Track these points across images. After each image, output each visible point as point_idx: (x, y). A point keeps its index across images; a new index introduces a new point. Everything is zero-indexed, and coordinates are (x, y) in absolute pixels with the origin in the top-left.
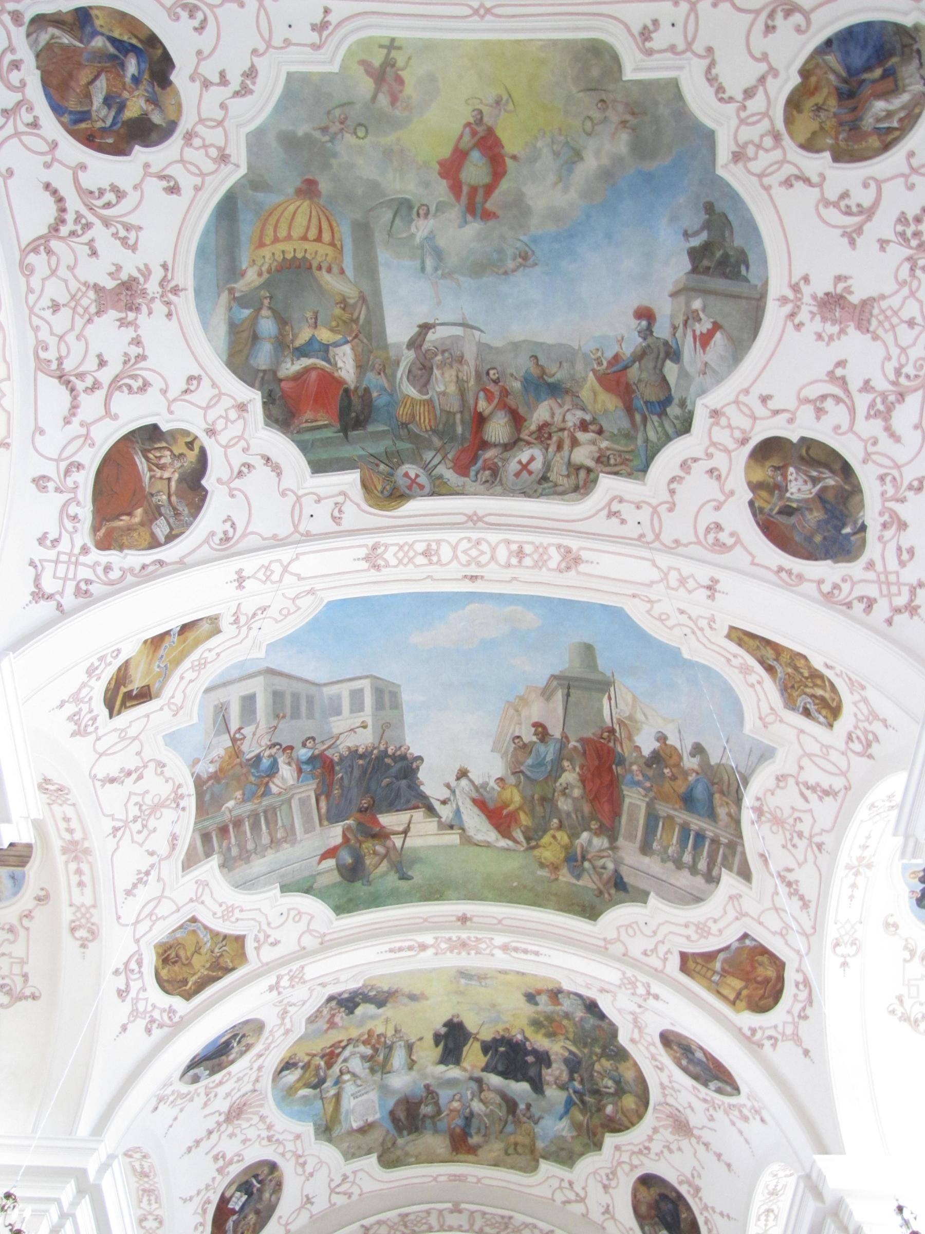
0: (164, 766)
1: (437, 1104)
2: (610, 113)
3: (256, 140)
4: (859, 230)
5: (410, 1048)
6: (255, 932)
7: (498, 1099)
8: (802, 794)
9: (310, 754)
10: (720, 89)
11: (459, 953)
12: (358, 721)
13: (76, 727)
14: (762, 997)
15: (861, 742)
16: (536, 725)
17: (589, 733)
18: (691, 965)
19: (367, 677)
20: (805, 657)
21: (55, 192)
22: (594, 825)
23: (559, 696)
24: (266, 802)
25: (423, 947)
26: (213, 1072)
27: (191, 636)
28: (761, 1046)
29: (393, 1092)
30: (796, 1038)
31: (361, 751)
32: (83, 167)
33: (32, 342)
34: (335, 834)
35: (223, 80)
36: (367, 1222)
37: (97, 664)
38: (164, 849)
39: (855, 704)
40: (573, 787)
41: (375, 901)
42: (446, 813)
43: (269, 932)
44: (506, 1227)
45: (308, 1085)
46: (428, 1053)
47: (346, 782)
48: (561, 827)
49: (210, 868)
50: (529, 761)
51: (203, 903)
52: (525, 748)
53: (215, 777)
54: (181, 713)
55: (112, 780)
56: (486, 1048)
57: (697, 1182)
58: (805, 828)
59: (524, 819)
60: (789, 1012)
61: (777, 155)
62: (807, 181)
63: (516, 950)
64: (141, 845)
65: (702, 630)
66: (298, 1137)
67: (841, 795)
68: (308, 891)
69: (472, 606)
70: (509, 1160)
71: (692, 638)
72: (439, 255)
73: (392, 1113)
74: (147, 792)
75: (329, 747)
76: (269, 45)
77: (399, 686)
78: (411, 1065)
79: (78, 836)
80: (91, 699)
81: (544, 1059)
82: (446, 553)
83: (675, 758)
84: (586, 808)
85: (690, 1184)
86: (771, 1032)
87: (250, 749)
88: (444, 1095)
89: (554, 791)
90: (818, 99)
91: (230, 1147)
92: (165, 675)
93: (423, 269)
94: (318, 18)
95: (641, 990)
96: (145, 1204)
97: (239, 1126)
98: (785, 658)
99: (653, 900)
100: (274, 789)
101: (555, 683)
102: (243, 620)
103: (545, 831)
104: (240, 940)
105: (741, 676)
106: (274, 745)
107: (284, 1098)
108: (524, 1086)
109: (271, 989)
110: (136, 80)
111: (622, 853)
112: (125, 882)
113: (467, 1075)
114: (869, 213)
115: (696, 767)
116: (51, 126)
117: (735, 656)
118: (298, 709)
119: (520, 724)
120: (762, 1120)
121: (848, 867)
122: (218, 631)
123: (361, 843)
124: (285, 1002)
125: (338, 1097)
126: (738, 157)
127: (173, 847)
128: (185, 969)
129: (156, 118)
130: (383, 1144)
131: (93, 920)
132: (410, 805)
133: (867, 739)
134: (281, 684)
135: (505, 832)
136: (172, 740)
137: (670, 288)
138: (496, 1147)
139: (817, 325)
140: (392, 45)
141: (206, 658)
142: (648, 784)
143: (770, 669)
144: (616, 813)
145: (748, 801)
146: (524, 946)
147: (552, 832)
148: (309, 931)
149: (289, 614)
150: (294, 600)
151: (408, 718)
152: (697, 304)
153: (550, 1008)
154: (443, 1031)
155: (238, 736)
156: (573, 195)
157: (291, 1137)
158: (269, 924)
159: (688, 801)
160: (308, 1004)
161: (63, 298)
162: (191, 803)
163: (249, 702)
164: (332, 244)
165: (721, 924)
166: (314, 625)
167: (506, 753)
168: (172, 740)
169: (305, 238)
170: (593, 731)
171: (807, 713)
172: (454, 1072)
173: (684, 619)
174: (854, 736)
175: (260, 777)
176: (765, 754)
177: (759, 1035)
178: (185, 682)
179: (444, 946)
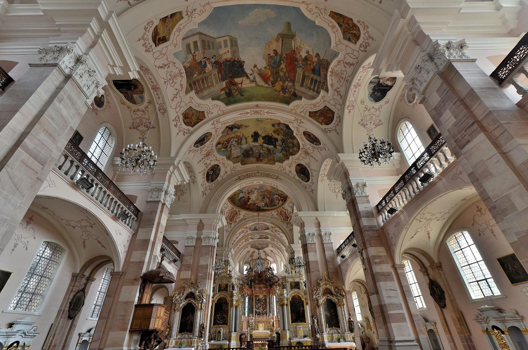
0: (175, 63)
1: (253, 151)
5: (246, 139)
6: (207, 110)
7: (266, 150)
8: (344, 66)
13: (146, 49)
14: (328, 121)
15: (364, 47)
16: (274, 50)
18: (312, 114)
19: (228, 36)
20: (352, 19)
22: (289, 79)
23: (281, 40)
24: (205, 75)
25: (248, 113)
26: (201, 145)
27: (175, 18)
28: (327, 132)
29: (243, 149)
30: (335, 130)
31: (228, 60)
34: (224, 84)
36: (239, 176)
37: (147, 26)
38: (180, 88)
39: (364, 34)
40: (284, 69)
41: (235, 102)
42: (251, 77)
43: (210, 110)
44: (269, 175)
45: (223, 148)
46: (250, 140)
47: (225, 69)
48: (281, 80)
49: (193, 93)
50: (272, 62)
51: (192, 103)
53: (190, 67)
54: (177, 46)
55: (161, 67)
56: (263, 138)
57: (310, 164)
58: (344, 76)
59: (271, 79)
60: (334, 124)
63: (269, 113)
64: (173, 87)
65: (322, 13)
66: (223, 159)
67: (355, 65)
68: (218, 100)
70: (269, 163)
73: (243, 153)
74: (172, 71)
78: (247, 143)
79: (155, 84)
80: (148, 39)
81: (276, 140)
84: (287, 75)
85: (308, 165)
86: (330, 129)
87: (199, 59)
88: (254, 149)
89: (279, 70)
91: (208, 162)
92: (170, 34)
95: (299, 121)
96: (191, 174)
97: (209, 157)
98: (346, 20)
99: (303, 99)
100: (207, 71)
102: (189, 14)
103: (276, 82)
104: (203, 112)
105: (332, 29)
106: (205, 58)
107: (218, 151)
108: (272, 146)
109: (212, 124)
111: (296, 87)
112: (171, 97)
113: (259, 144)
115: (316, 61)
117: (331, 22)
118: (210, 46)
120: (325, 150)
121: (354, 86)
122: (182, 18)
123: (230, 86)
124: (216, 128)
125: (231, 150)
127: (182, 88)
128: (190, 120)
130: (241, 160)
131: (164, 107)
132: (242, 76)
133: (366, 46)
134: (204, 38)
135: (266, 82)
136: (176, 55)
138: (266, 160)
141: (180, 28)
142: (303, 67)
143: (340, 26)
144: (295, 76)
145: (330, 70)
147: (278, 82)
148: (220, 110)
149: (203, 12)
151: (240, 49)
153: (278, 128)
154: (253, 134)
155: (194, 55)
157: (221, 159)
158: (210, 108)
159: (314, 71)
160: (222, 129)
162: (184, 75)
163: (195, 43)
165: (319, 104)
166: (211, 17)
167: (266, 59)
168: (176, 55)
171: (349, 40)
172: (256, 144)
173: (317, 10)
174: (362, 45)
175: (202, 67)
176: (336, 55)
177: (327, 130)
178: (176, 36)
179: (252, 113)
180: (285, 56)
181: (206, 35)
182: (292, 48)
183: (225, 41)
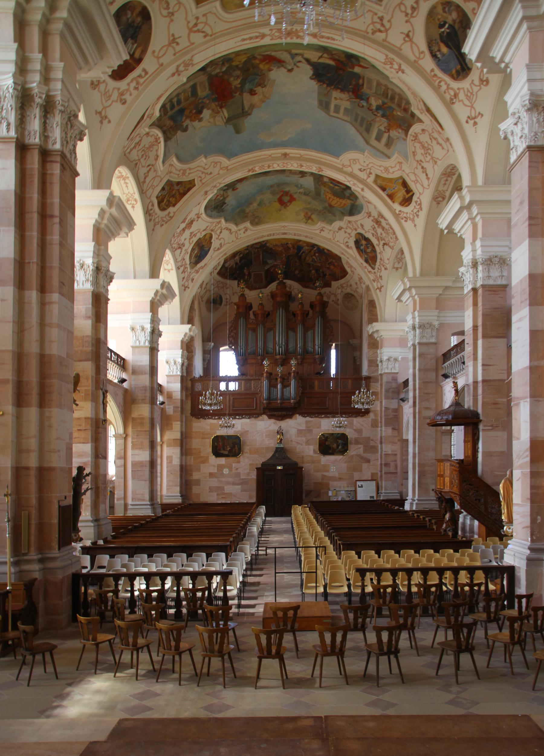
3: (341, 219)
9: (362, 101)
11: (292, 29)
16: (255, 94)
23: (246, 108)
27: (384, 184)
31: (339, 91)
35: (346, 232)
48: (237, 66)
52: (259, 85)
55: (427, 175)
63: (257, 37)
72: (297, 186)
94: (322, 232)
101: (249, 112)
106: (375, 115)
116: (379, 256)
129: (361, 237)
136: (406, 157)
140: (306, 223)
146: (252, 41)
150: (350, 166)
151: (315, 95)
161: (389, 238)
181: (361, 134)
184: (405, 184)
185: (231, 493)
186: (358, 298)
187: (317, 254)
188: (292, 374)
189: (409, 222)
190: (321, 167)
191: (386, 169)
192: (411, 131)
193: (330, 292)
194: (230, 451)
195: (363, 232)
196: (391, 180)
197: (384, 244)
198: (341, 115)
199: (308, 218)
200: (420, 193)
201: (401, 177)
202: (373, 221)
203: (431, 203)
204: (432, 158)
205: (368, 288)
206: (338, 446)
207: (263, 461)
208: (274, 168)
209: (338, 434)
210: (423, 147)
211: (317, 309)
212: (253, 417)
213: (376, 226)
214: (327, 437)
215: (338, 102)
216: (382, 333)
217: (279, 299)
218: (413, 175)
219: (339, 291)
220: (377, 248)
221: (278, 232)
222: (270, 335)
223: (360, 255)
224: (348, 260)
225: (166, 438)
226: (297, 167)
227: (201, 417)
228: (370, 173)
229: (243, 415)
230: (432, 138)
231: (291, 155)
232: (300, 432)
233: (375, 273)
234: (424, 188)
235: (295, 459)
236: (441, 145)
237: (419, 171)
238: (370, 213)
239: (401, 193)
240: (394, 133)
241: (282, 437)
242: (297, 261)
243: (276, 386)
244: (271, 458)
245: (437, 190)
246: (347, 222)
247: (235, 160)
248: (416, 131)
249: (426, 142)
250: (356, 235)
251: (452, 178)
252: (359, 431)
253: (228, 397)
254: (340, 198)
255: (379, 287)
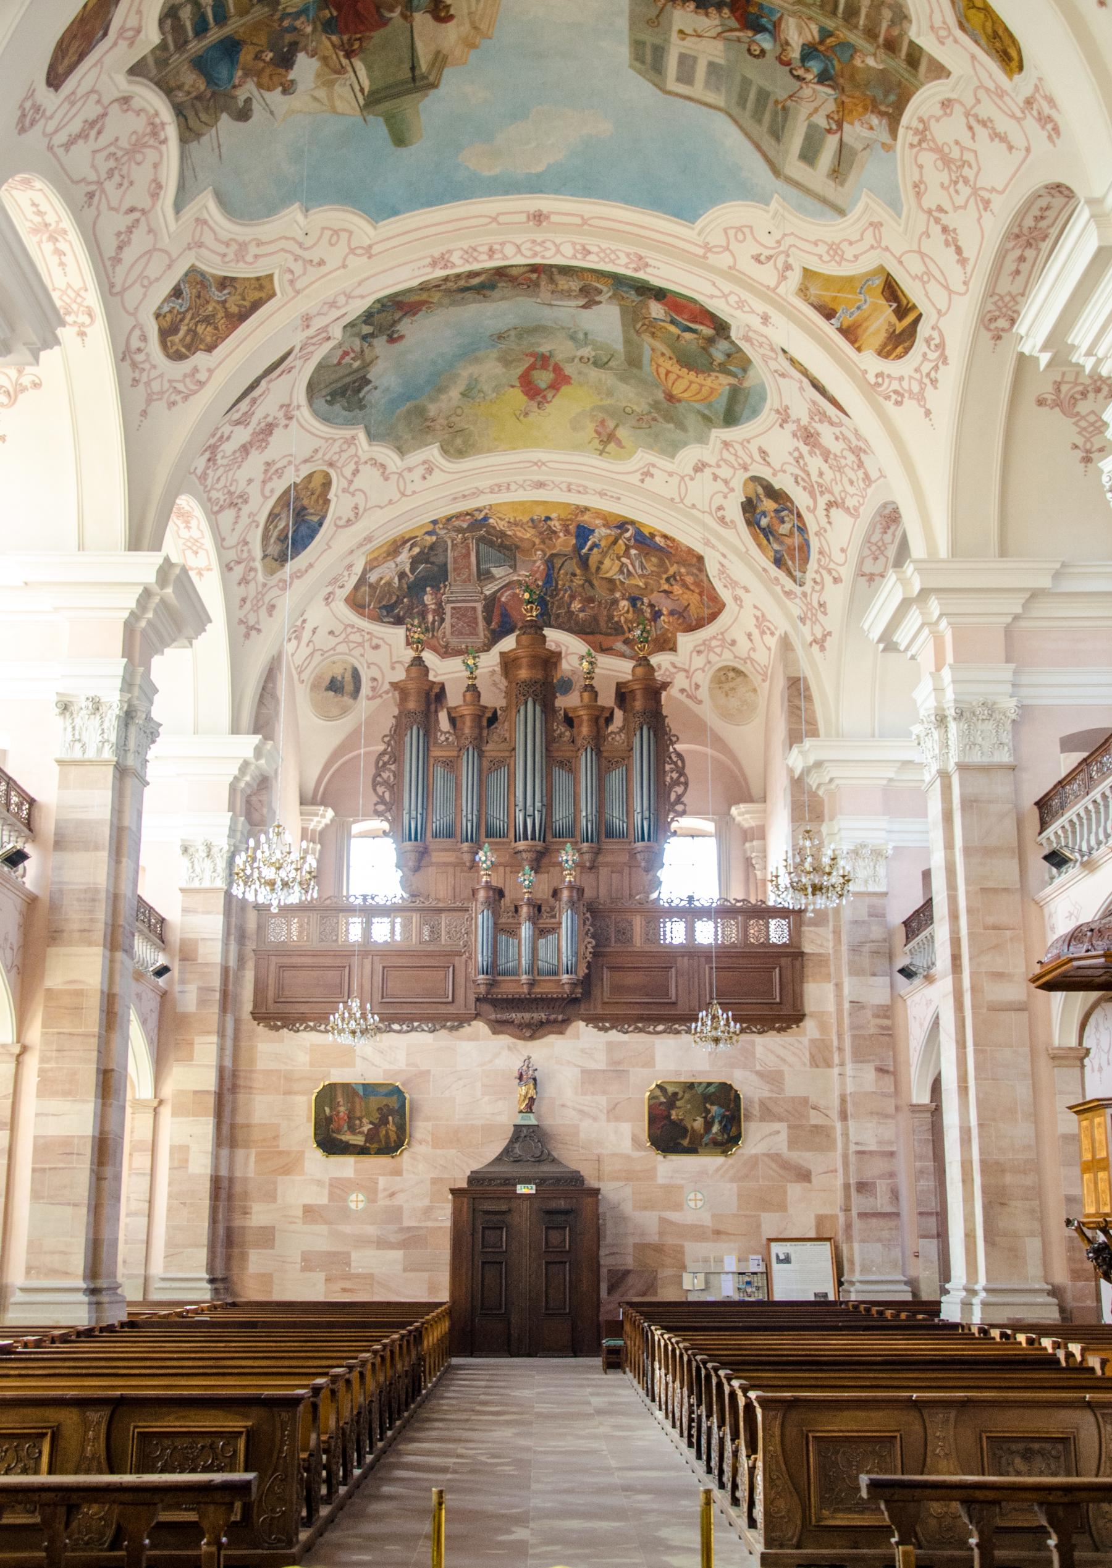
2: (445, 422)
3: (702, 440)
4: (266, 471)
9: (758, 37)
10: (374, 462)
12: (689, 42)
16: (450, 18)
17: (378, 35)
19: (669, 93)
21: (828, 516)
23: (424, 66)
24: (830, 24)
27: (827, 296)
32: (808, 508)
33: (869, 491)
35: (715, 477)
37: (894, 397)
61: (327, 458)
62: (306, 461)
69: (540, 169)
71: (300, 237)
72: (573, 338)
75: (732, 30)
76: (682, 478)
77: (631, 66)
82: (568, 250)
83: (265, 80)
90: (314, 497)
93: (586, 334)
94: (648, 479)
98: (222, 324)
100: (814, 28)
106: (798, 78)
110: (764, 514)
114: (264, 482)
116: (814, 544)
118: (758, 100)
119: (470, 13)
126: (353, 438)
129: (760, 490)
134: (768, 142)
136: (894, 205)
137: (379, 361)
139: (270, 419)
140: (601, 453)
142: (286, 23)
143: (225, 283)
145: (171, 132)
150: (727, 248)
151: (623, 23)
152: (356, 364)
155: (834, 127)
156: (465, 374)
161: (845, 481)
163: (809, 155)
164: (658, 366)
166: (716, 196)
169: (679, 377)
170: (373, 41)
171: (177, 293)
173: (315, 255)
180: (388, 15)
181: (758, 147)
182: (364, 60)
183: (686, 75)
184: (891, 290)
185: (371, 1276)
186: (756, 680)
187: (633, 552)
188: (565, 894)
189: (909, 404)
190: (643, 252)
191: (835, 250)
192: (908, 117)
193: (674, 665)
194: (371, 1136)
195: (765, 473)
196: (847, 282)
197: (830, 505)
198: (698, 89)
199: (607, 439)
200: (939, 312)
201: (882, 268)
202: (795, 435)
203: (976, 332)
204: (975, 191)
205: (786, 644)
206: (708, 1125)
207: (476, 1166)
208: (505, 258)
209: (709, 1084)
210: (947, 161)
211: (638, 705)
212: (443, 1027)
213: (805, 449)
214: (675, 1094)
215: (689, 45)
216: (832, 771)
217: (524, 674)
218: (917, 257)
219: (699, 661)
220: (808, 518)
221: (520, 479)
222: (497, 782)
223: (759, 545)
224: (724, 561)
225: (168, 1090)
226: (574, 257)
227: (282, 1027)
228: (788, 267)
229: (412, 1020)
230: (976, 122)
231: (553, 218)
232: (589, 1077)
233: (805, 595)
234: (950, 292)
235: (574, 1166)
236: (1003, 138)
237: (935, 245)
238: (787, 408)
239: (883, 318)
240: (855, 132)
241: (532, 1093)
242: (578, 571)
243: (513, 932)
244: (499, 1159)
245: (991, 292)
246: (719, 445)
247: (392, 226)
248: (924, 112)
249: (957, 143)
250: (745, 484)
251: (1039, 250)
252: (773, 1078)
253: (367, 962)
254: (698, 371)
255: (819, 636)
